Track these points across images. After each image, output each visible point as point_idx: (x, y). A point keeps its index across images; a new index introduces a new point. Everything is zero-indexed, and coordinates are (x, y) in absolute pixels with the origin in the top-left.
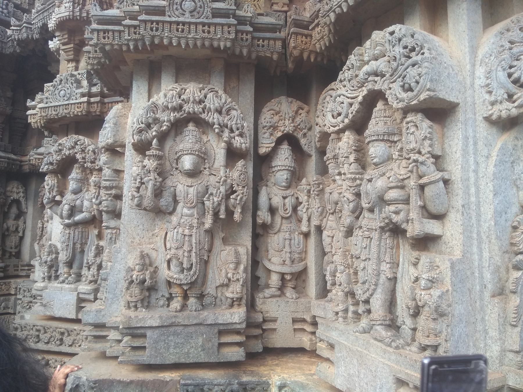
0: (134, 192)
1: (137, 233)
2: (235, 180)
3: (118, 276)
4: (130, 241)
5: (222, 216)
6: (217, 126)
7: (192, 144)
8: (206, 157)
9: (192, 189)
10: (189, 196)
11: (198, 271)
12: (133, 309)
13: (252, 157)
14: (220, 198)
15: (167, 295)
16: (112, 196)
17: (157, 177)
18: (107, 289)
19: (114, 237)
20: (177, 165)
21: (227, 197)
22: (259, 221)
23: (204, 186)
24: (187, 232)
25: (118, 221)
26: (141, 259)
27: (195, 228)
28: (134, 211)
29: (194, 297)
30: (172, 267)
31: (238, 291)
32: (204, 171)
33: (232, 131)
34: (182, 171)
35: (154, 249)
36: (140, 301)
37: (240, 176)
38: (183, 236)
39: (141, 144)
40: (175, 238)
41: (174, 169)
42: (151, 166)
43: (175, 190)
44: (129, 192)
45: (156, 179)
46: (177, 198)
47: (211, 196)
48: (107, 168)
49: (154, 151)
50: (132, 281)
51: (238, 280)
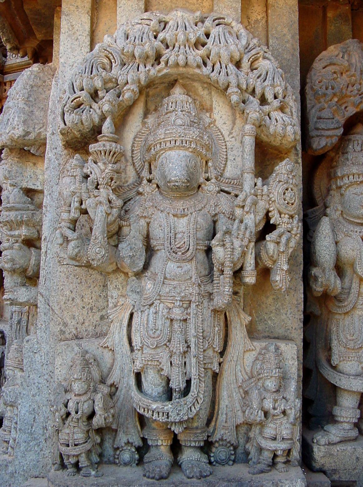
0: (65, 229)
1: (70, 313)
2: (274, 201)
3: (37, 398)
4: (57, 329)
5: (250, 278)
6: (236, 90)
7: (183, 127)
8: (209, 156)
9: (183, 221)
10: (179, 236)
11: (201, 396)
12: (71, 470)
13: (300, 155)
14: (246, 240)
15: (138, 442)
16: (20, 240)
17: (113, 197)
18: (16, 423)
19: (25, 318)
20: (151, 173)
21: (261, 236)
22: (318, 289)
23: (209, 215)
24: (177, 313)
25: (33, 290)
26: (83, 369)
27: (193, 306)
28: (63, 269)
29: (195, 447)
30: (145, 385)
31: (285, 436)
32: (205, 184)
33: (263, 101)
34: (161, 184)
35: (107, 347)
36: (84, 455)
37: (284, 194)
38: (168, 322)
39: (80, 131)
40: (151, 325)
41: (145, 182)
42: (101, 175)
43: (148, 224)
44: (56, 229)
45: (110, 202)
46: (153, 243)
47: (227, 236)
48: (12, 185)
49: (108, 144)
50: (68, 414)
51: (284, 412)
